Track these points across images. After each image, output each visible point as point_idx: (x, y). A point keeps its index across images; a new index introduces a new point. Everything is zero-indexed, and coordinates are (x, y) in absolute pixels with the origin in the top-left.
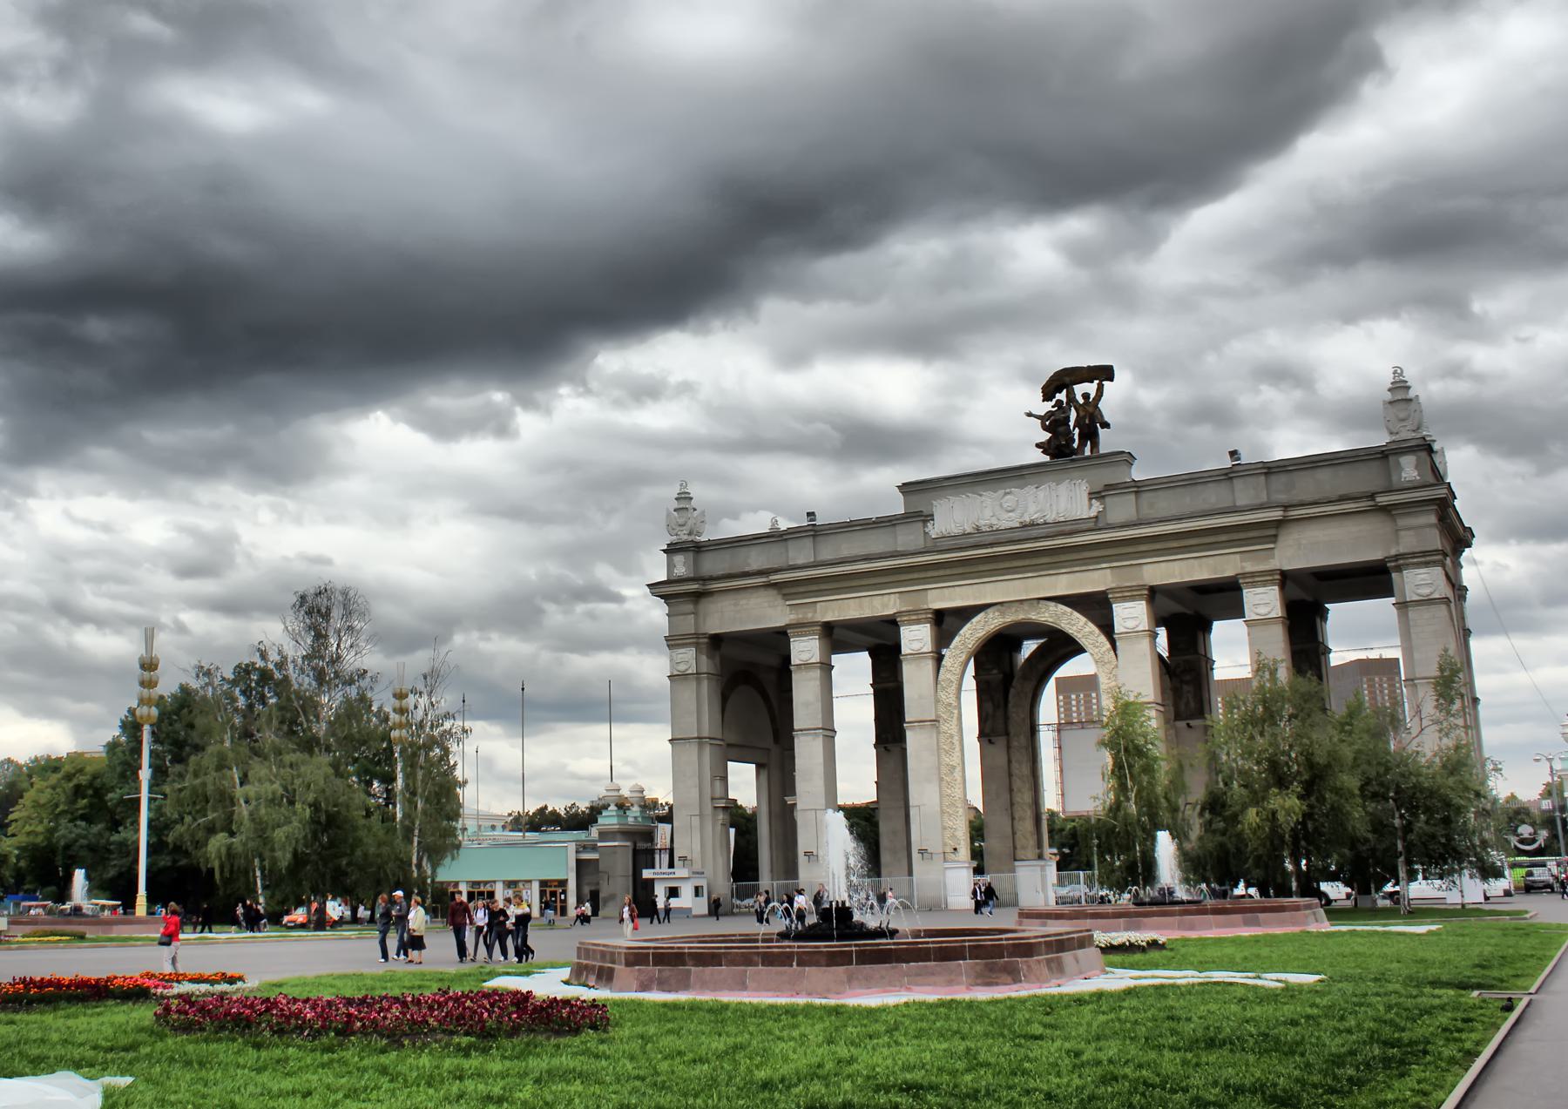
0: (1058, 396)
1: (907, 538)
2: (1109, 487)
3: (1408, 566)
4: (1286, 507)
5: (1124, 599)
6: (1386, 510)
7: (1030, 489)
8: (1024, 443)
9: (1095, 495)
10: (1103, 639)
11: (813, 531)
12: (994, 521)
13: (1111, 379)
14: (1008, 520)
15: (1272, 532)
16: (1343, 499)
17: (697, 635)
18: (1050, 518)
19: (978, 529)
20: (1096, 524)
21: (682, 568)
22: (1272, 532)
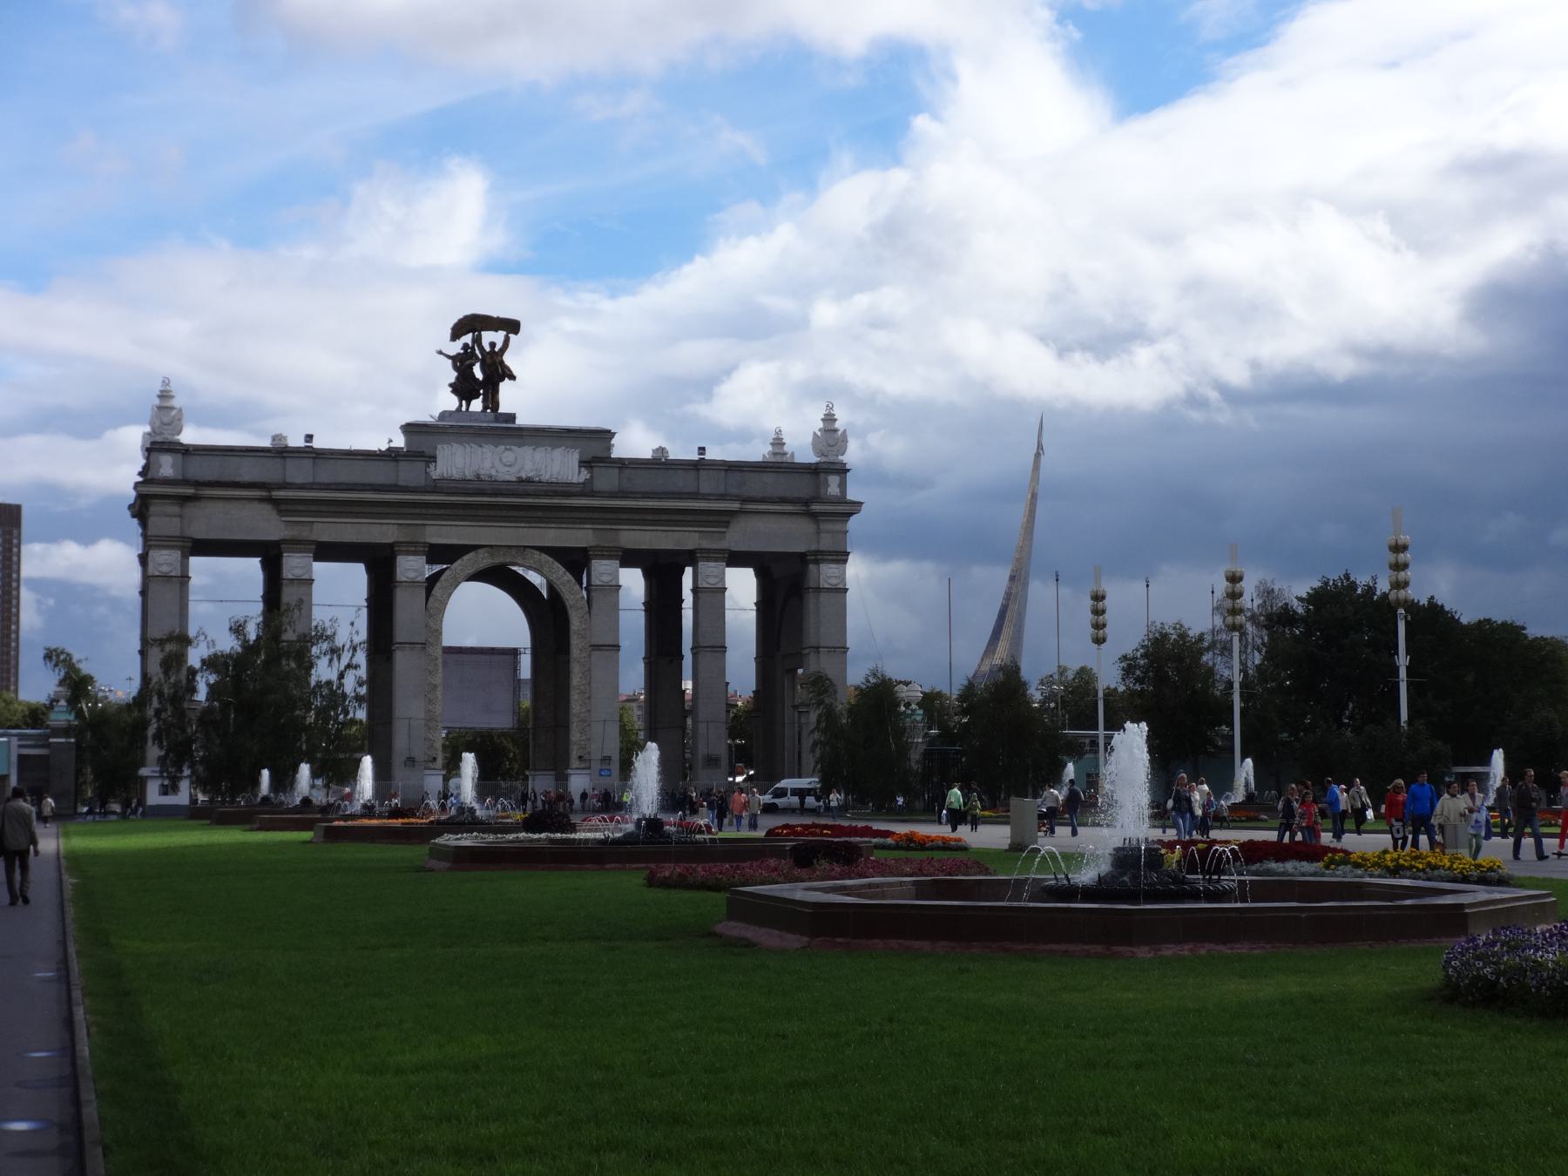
3: (824, 561)
4: (745, 500)
5: (603, 557)
11: (311, 454)
12: (493, 473)
13: (516, 332)
14: (506, 474)
17: (183, 538)
18: (546, 477)
19: (478, 476)
20: (586, 490)
21: (167, 466)
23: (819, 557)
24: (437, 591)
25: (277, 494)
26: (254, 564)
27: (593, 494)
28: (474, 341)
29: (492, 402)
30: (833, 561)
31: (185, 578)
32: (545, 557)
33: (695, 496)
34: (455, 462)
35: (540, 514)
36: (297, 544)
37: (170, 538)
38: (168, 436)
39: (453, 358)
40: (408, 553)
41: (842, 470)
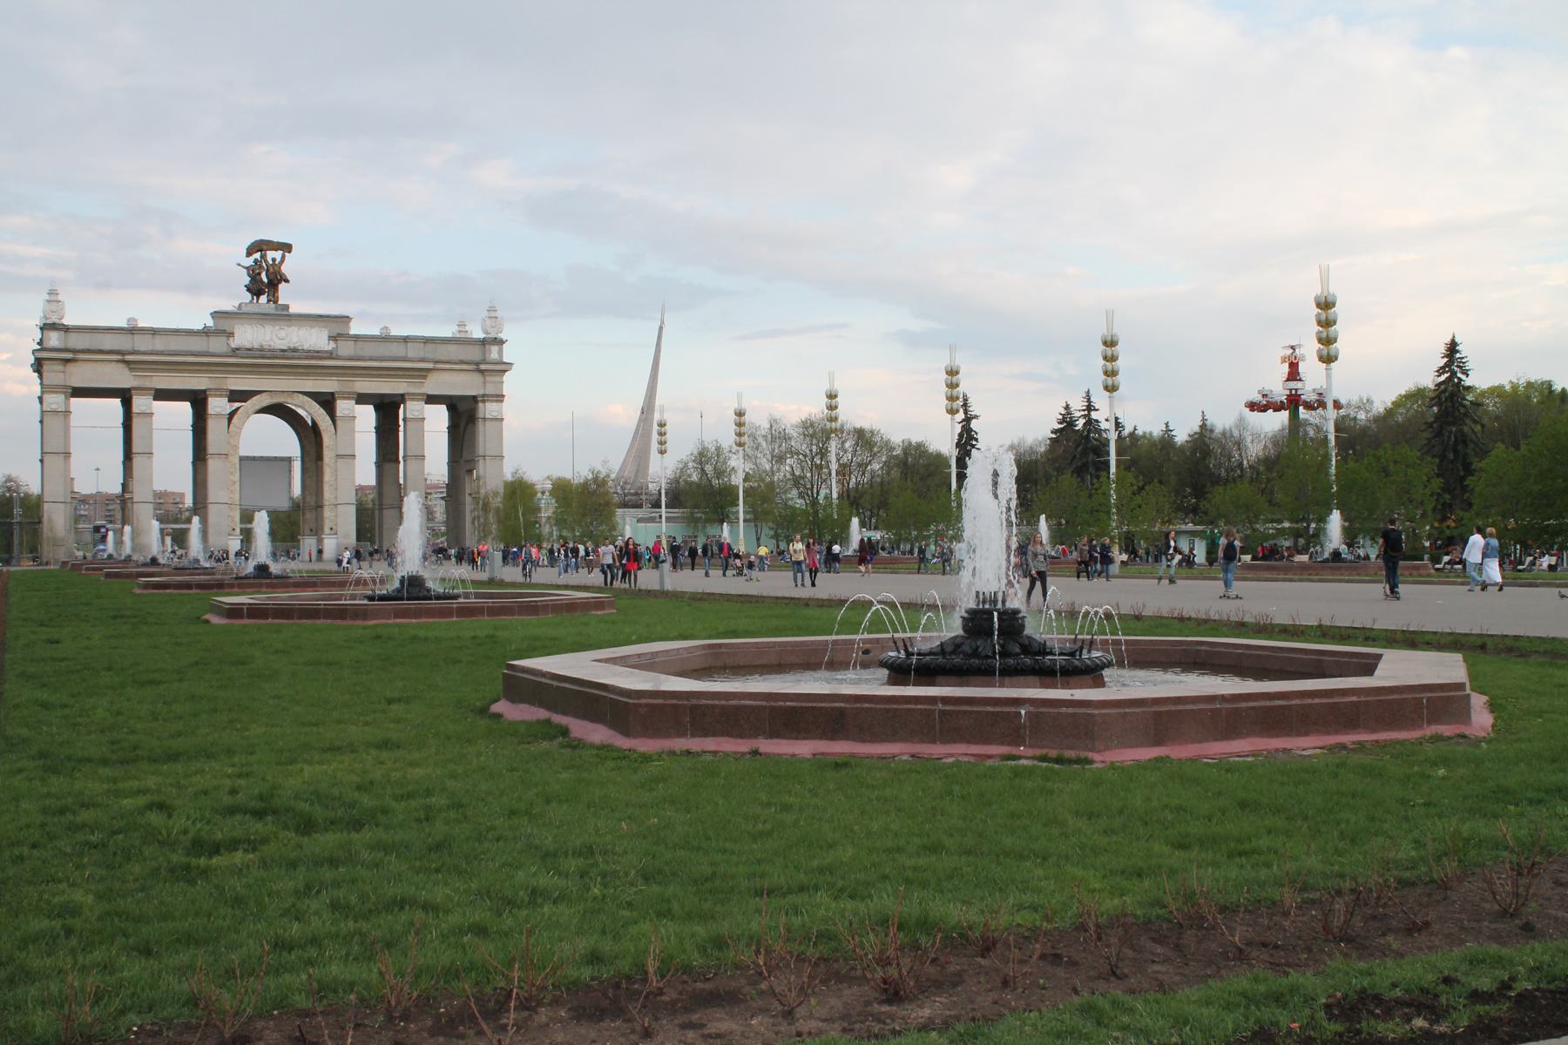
1: (217, 345)
2: (340, 335)
6: (482, 372)
7: (294, 329)
9: (331, 338)
16: (462, 362)
20: (330, 355)
21: (54, 339)
23: (485, 398)
24: (235, 420)
25: (128, 358)
26: (117, 402)
27: (338, 358)
29: (274, 299)
31: (67, 413)
32: (306, 398)
33: (405, 359)
34: (247, 336)
36: (142, 390)
37: (57, 386)
38: (54, 319)
41: (500, 342)
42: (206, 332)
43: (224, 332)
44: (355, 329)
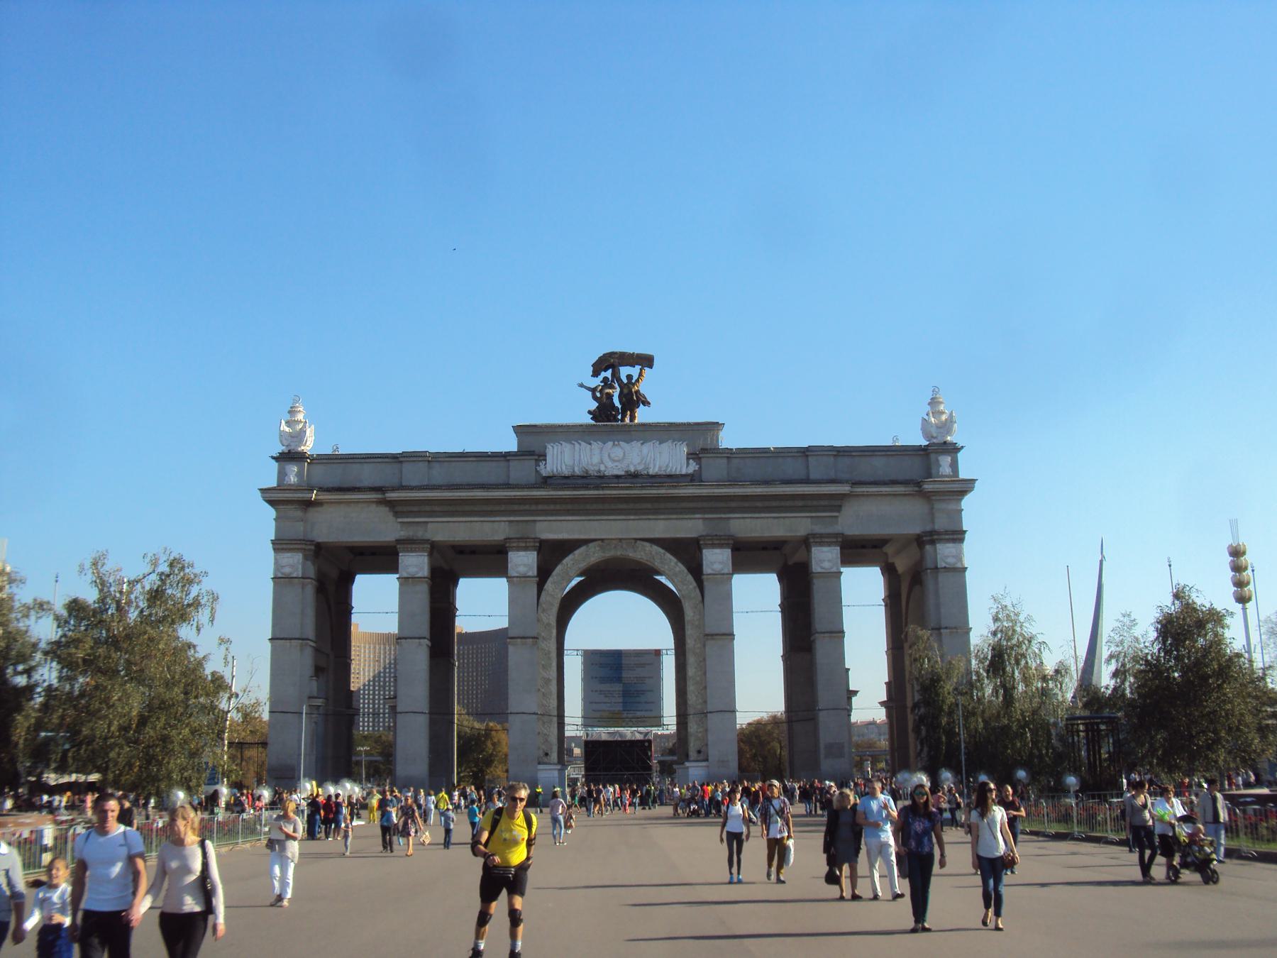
0: (603, 374)
2: (704, 450)
3: (940, 540)
5: (713, 546)
7: (636, 445)
8: (580, 410)
10: (690, 577)
12: (602, 468)
13: (651, 366)
14: (612, 468)
15: (838, 503)
20: (692, 479)
22: (838, 503)
28: (613, 375)
30: (948, 541)
35: (649, 506)
39: (593, 390)
40: (519, 549)
41: (953, 449)
42: (506, 456)
43: (531, 453)
44: (728, 440)
